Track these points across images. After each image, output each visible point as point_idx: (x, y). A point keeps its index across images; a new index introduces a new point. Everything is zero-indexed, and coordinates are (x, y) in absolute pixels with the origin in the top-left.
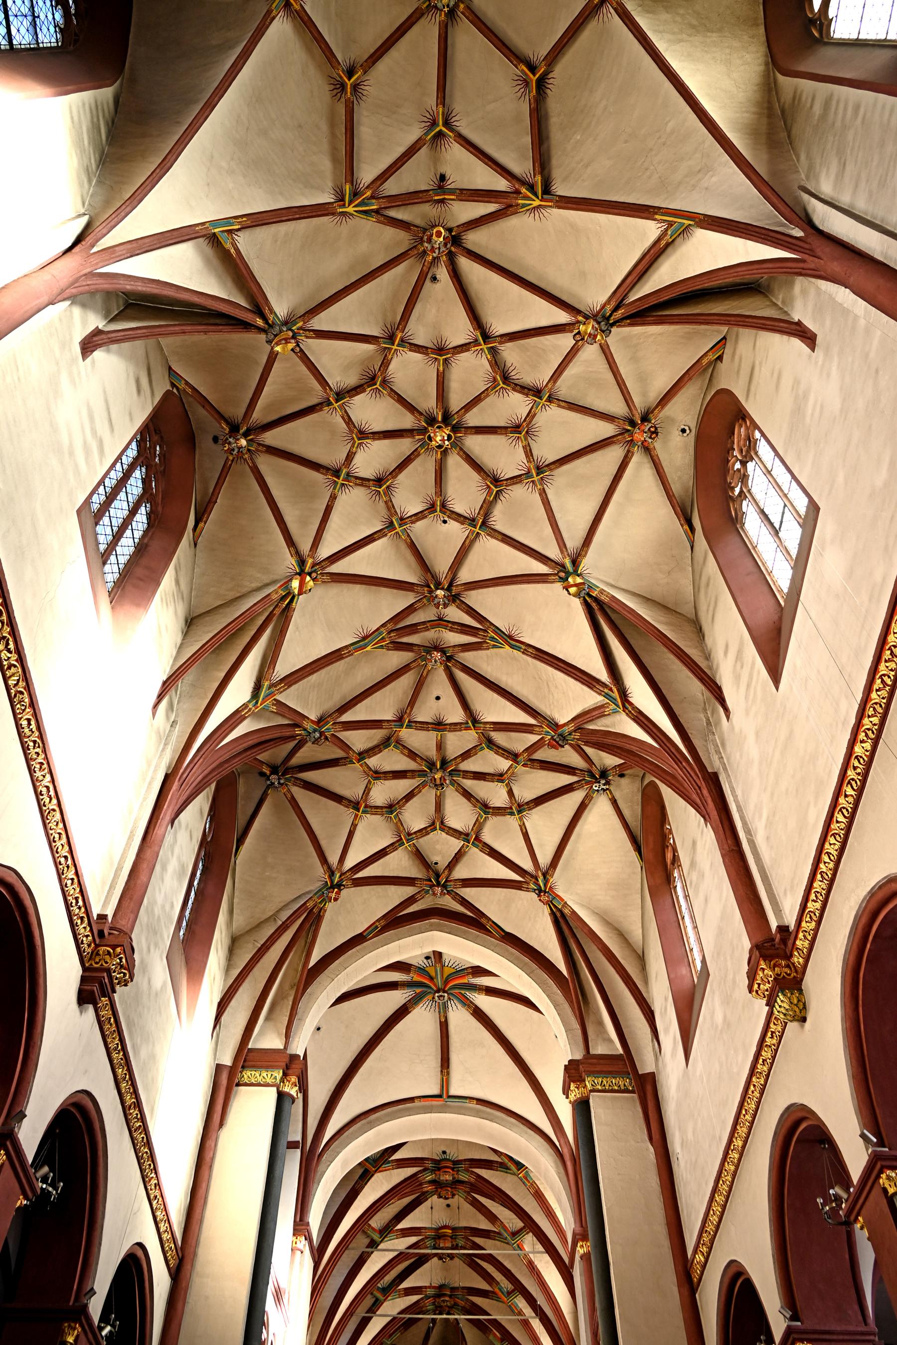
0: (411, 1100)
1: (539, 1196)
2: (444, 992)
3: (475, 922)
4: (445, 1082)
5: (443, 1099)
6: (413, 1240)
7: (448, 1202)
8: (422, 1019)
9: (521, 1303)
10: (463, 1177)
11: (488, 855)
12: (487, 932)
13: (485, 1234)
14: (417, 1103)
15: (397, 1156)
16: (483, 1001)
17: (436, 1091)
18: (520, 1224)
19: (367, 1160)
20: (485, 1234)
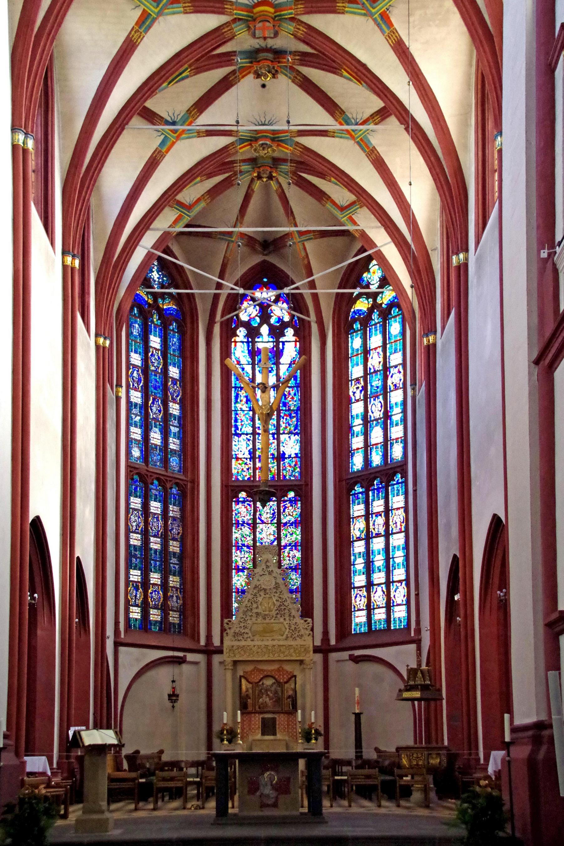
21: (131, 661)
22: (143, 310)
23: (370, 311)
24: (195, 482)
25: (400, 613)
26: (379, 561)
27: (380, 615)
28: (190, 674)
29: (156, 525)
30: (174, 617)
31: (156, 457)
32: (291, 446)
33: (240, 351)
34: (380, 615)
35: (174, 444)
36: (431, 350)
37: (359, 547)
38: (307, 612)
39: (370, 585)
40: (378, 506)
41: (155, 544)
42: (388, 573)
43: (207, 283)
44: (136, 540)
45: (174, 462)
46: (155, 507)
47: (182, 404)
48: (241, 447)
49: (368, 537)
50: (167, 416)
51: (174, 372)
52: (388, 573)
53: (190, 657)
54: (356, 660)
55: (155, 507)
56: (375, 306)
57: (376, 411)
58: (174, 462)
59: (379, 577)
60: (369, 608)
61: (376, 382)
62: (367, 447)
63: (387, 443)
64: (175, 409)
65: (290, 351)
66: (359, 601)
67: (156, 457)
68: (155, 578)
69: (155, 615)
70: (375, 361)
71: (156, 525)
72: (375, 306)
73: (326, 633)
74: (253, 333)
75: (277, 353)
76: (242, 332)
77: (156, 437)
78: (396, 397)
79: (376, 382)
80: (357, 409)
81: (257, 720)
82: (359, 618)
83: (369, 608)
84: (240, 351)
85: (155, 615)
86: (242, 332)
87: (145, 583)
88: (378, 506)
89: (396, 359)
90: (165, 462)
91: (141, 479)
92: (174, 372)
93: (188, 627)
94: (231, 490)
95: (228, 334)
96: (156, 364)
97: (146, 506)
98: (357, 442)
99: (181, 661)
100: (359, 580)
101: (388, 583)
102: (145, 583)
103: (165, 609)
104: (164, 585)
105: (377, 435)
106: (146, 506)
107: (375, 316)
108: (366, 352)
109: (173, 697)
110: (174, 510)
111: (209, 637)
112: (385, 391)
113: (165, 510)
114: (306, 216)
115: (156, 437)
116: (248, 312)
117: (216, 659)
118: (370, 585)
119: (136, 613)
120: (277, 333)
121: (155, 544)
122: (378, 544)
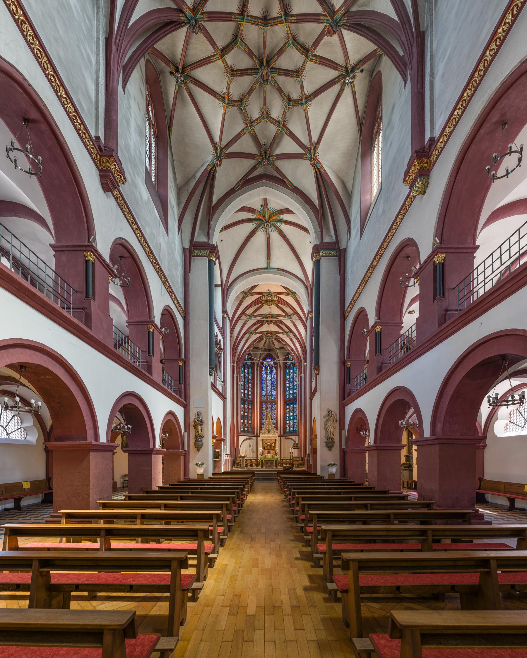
0: (257, 269)
1: (298, 303)
2: (269, 223)
3: (281, 181)
4: (269, 263)
5: (268, 269)
6: (260, 318)
7: (270, 306)
8: (260, 237)
9: (291, 335)
10: (274, 299)
11: (288, 135)
12: (286, 186)
13: (281, 316)
14: (259, 271)
15: (254, 291)
16: (284, 227)
17: (265, 266)
18: (292, 312)
19: (243, 292)
20: (281, 316)
21: (242, 438)
22: (244, 365)
23: (290, 365)
24: (254, 401)
25: (295, 429)
26: (291, 418)
27: (291, 429)
28: (253, 441)
29: (247, 410)
30: (250, 430)
31: (246, 396)
32: (274, 393)
33: (263, 372)
34: (291, 429)
35: (250, 393)
36: (301, 377)
37: (288, 415)
38: (277, 429)
39: (290, 423)
40: (291, 406)
41: (246, 414)
42: (293, 421)
43: (257, 360)
44: (242, 413)
45: (250, 396)
46: (246, 406)
47: (252, 384)
48: (264, 393)
49: (289, 413)
50: (249, 387)
51: (250, 377)
52: (293, 421)
53: (253, 438)
54: (287, 439)
55: (246, 406)
56: (291, 363)
57: (291, 386)
58: (250, 396)
59: (291, 421)
60: (289, 428)
61: (291, 380)
62: (289, 394)
63: (293, 393)
64: (250, 385)
65: (274, 372)
66: (288, 426)
67: (246, 396)
68: (246, 421)
69: (246, 429)
70: (291, 375)
71: (247, 410)
72: (291, 363)
73: (281, 433)
74: (266, 368)
75: (271, 373)
76: (264, 368)
77: (246, 392)
78: (295, 383)
79: (291, 380)
80: (288, 385)
81: (266, 451)
82: (288, 430)
83: (289, 428)
84: (263, 372)
85: (246, 429)
86: (264, 368)
87: (244, 422)
88: (291, 406)
89: (295, 375)
90: (248, 397)
91: (243, 401)
92: (250, 377)
93: (252, 432)
94: (261, 403)
95: (261, 369)
96: (246, 376)
97: (244, 406)
98: (287, 392)
99: (251, 439)
100: (288, 422)
101: (293, 422)
102: (244, 422)
103: (248, 428)
104: (248, 423)
105: (291, 391)
106: (244, 406)
107: (291, 366)
108: (289, 373)
109: (250, 446)
110: (250, 407)
111: (257, 433)
112: (293, 382)
113: (248, 407)
114: (277, 345)
115: (246, 392)
116: (266, 363)
117: (258, 438)
118: (290, 423)
119: (242, 429)
120: (271, 368)
121: (246, 414)
122: (291, 414)
